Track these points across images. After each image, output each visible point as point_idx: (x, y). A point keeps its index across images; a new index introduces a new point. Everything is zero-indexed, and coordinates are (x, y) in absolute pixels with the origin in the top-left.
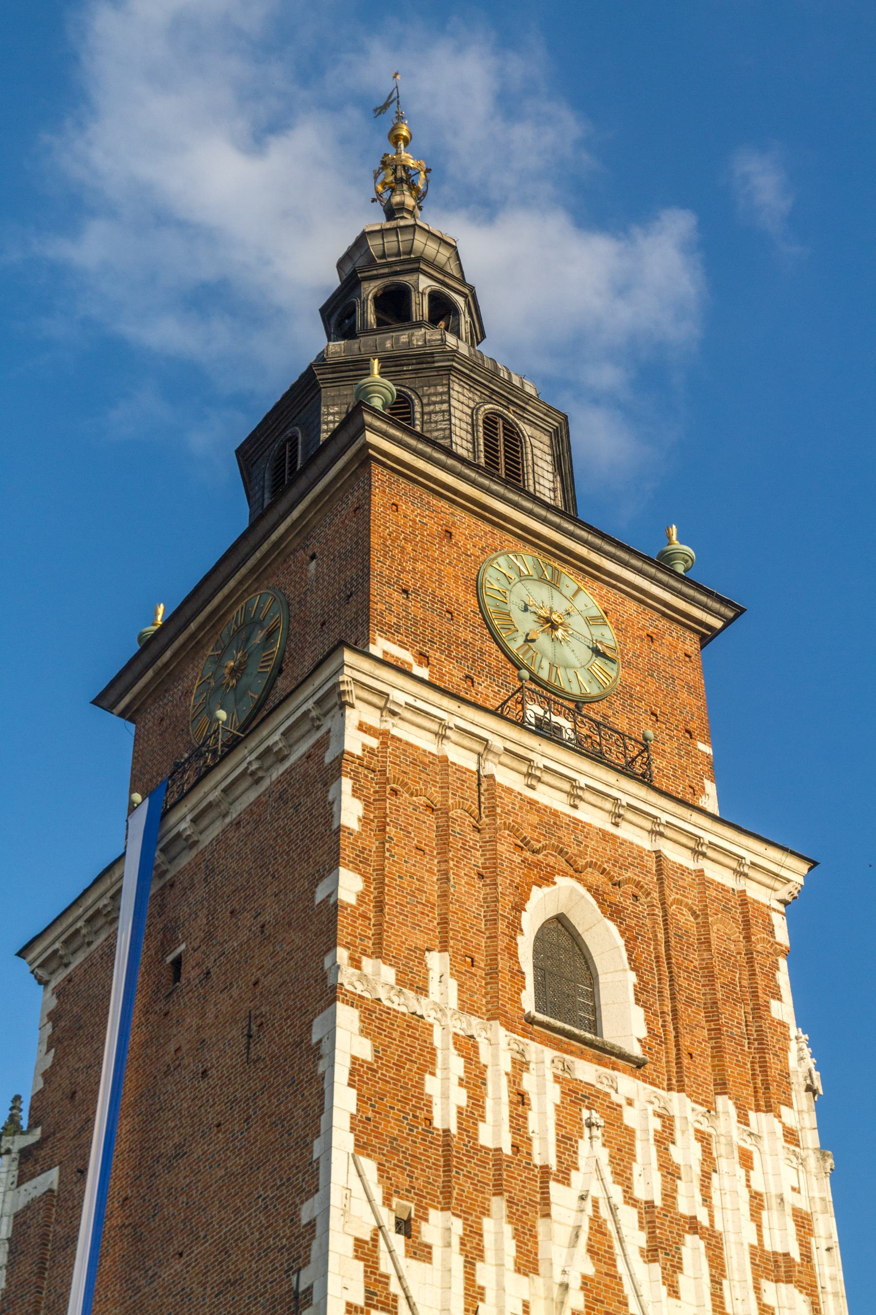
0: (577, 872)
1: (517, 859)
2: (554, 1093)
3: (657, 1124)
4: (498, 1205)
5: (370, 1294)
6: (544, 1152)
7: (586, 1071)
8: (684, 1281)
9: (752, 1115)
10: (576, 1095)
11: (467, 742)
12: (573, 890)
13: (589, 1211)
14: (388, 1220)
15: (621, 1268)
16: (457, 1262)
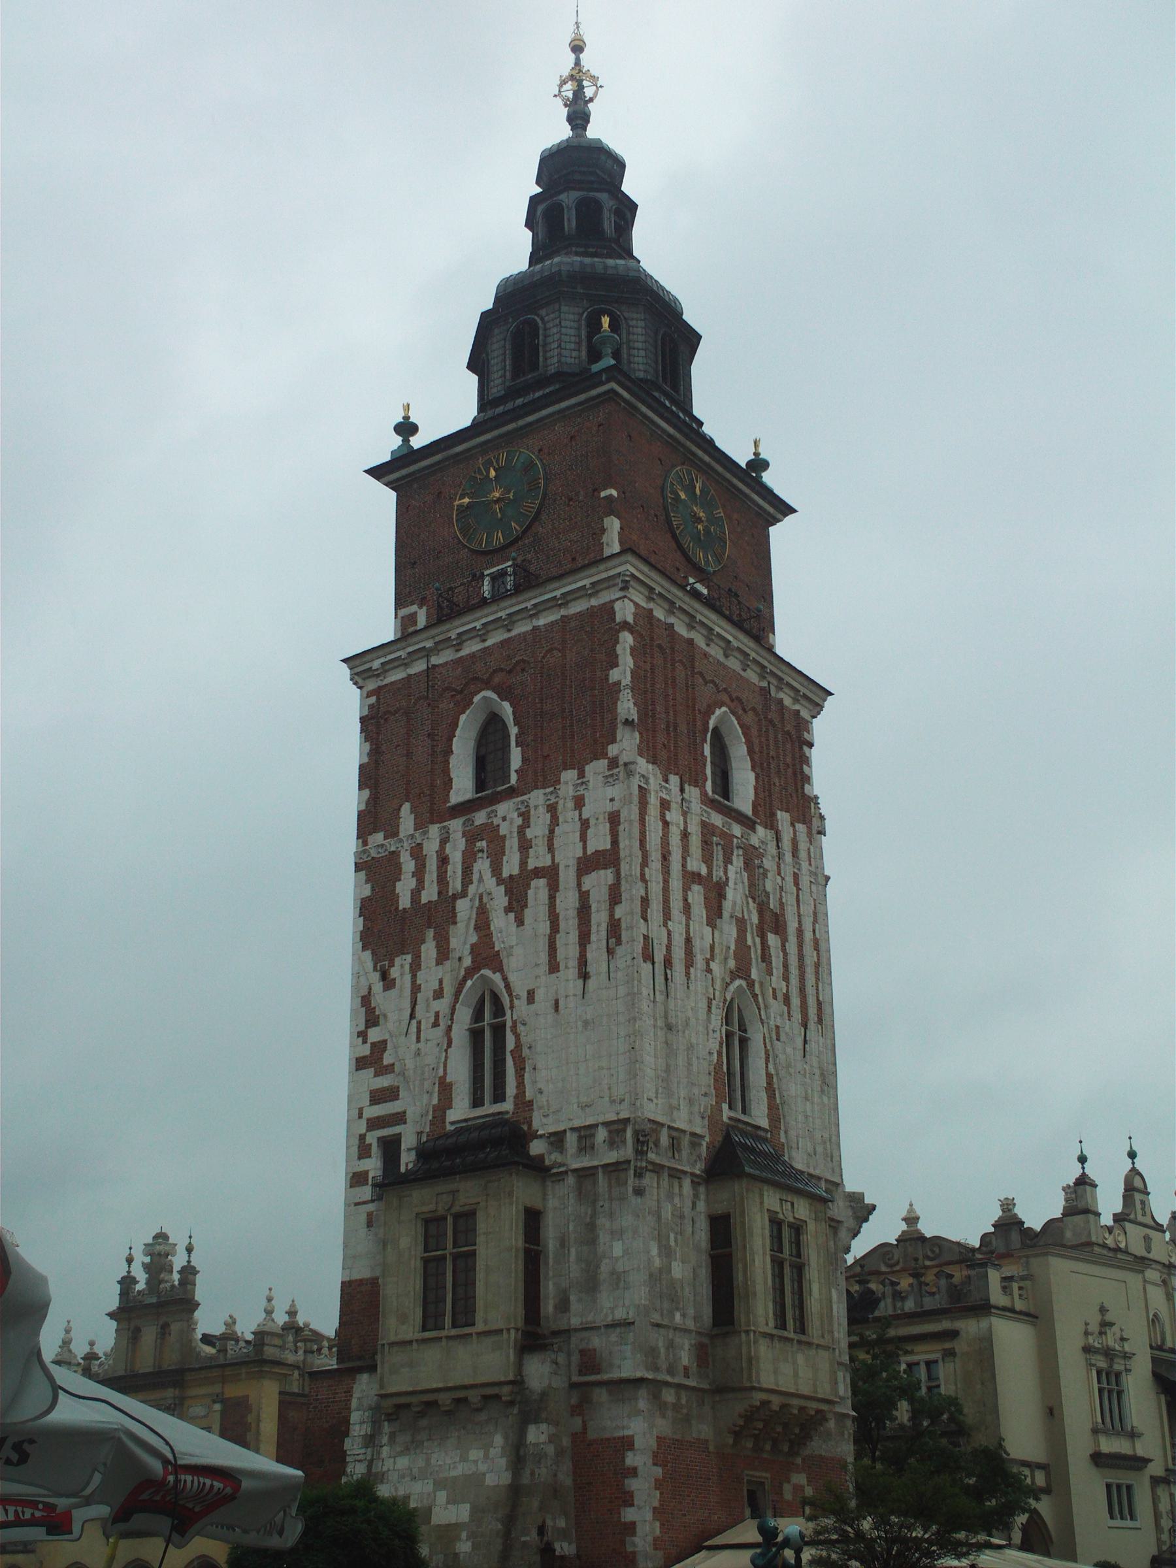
0: (487, 685)
1: (452, 705)
2: (461, 844)
3: (520, 821)
4: (430, 934)
5: (367, 1021)
6: (456, 884)
7: (480, 818)
8: (527, 911)
9: (587, 768)
10: (472, 837)
11: (420, 655)
12: (484, 698)
13: (477, 903)
14: (376, 976)
15: (492, 928)
16: (408, 977)
